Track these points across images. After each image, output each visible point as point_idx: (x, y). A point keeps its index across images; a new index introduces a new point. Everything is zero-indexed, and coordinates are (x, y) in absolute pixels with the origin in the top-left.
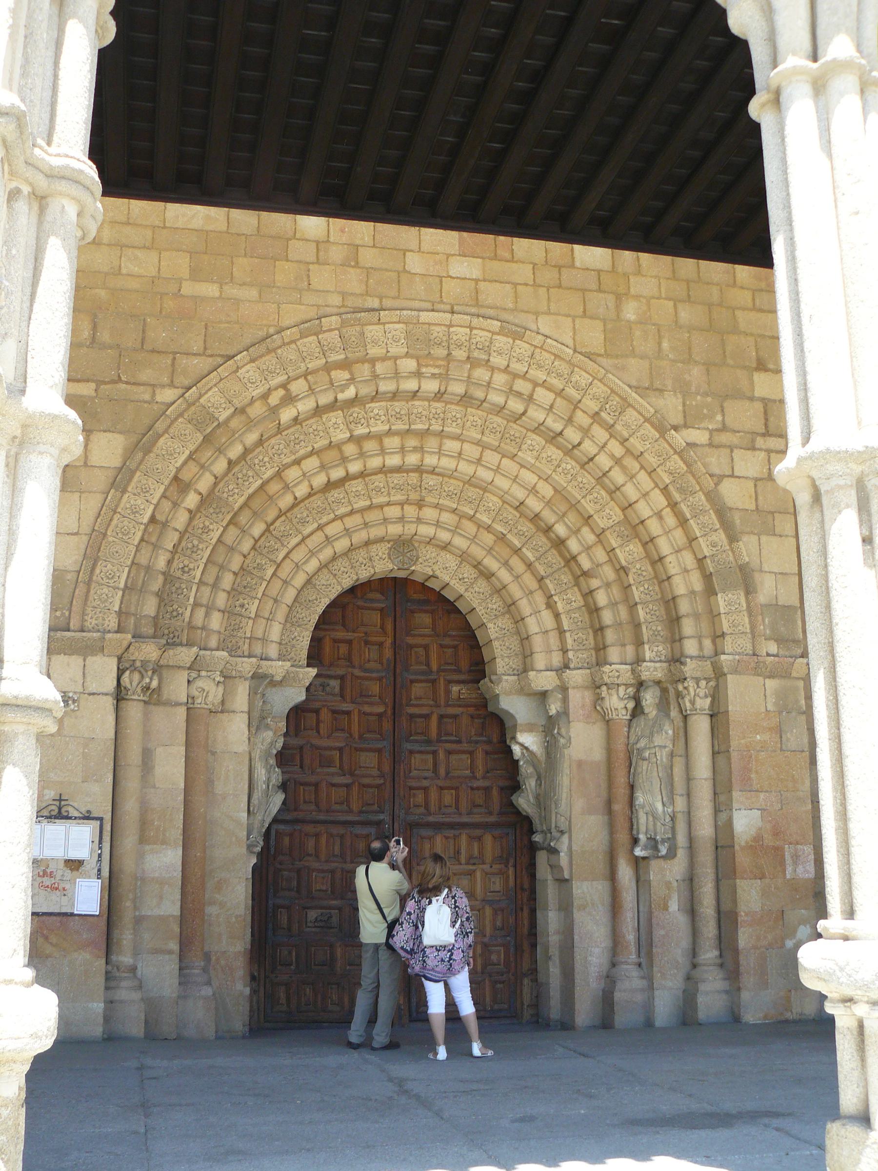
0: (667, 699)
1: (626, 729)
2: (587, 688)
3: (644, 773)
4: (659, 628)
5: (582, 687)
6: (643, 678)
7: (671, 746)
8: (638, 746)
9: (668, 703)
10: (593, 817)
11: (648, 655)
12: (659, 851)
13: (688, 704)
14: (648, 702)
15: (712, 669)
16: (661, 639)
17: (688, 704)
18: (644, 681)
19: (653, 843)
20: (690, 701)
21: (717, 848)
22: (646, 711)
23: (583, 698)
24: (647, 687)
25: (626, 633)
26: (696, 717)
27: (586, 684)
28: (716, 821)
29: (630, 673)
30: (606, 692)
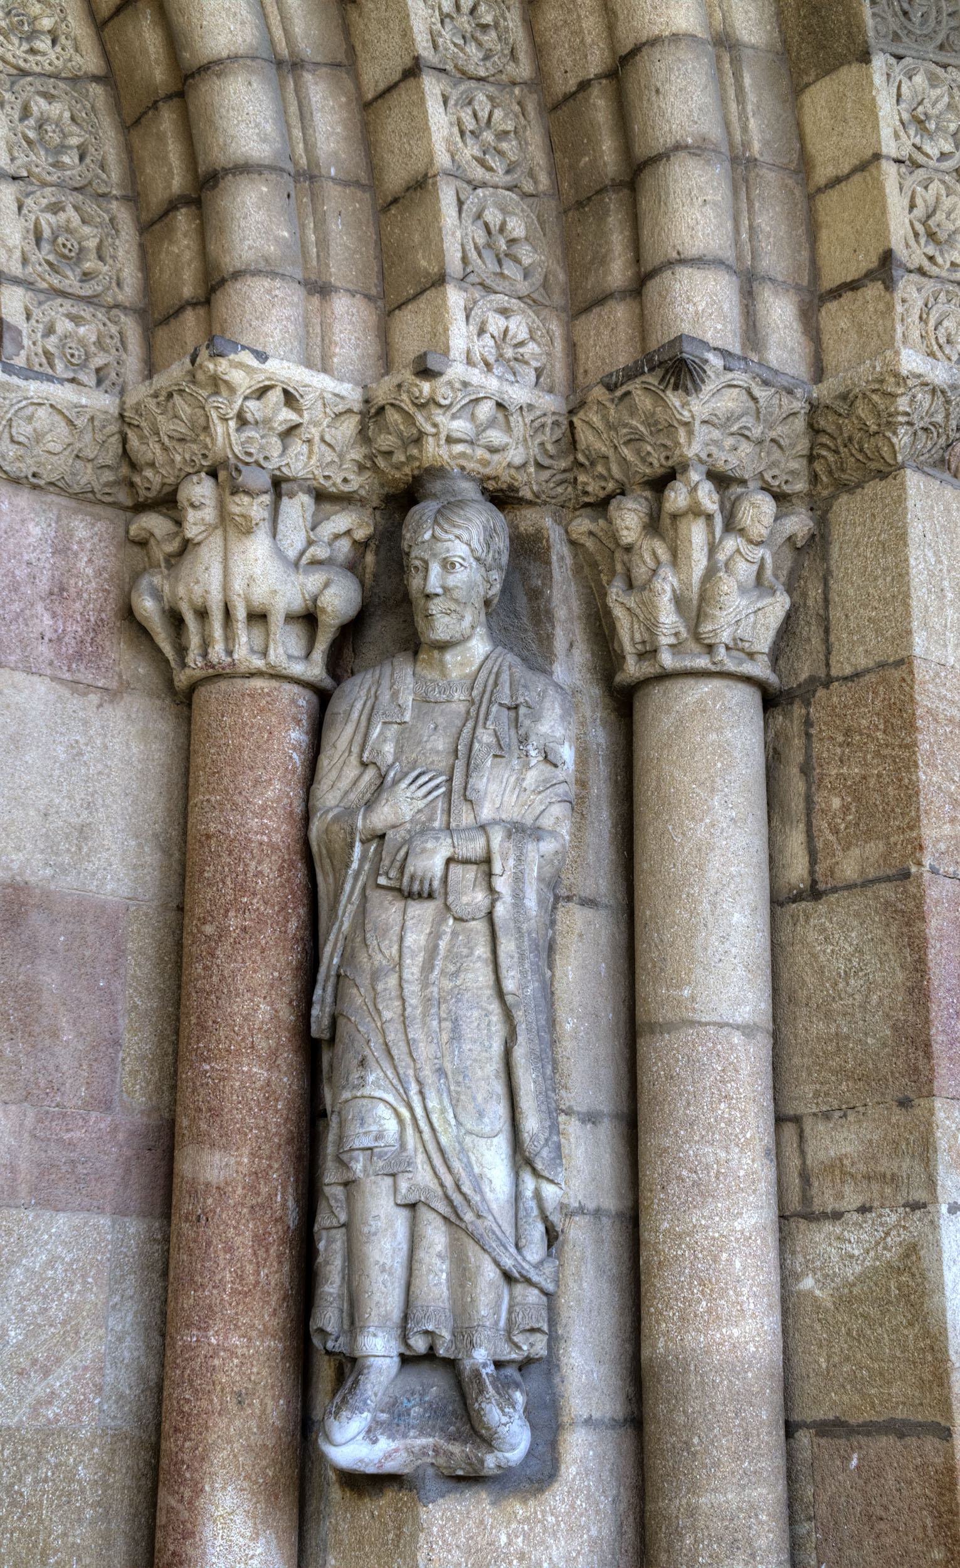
0: (535, 595)
1: (297, 736)
2: (85, 498)
3: (412, 969)
4: (517, 227)
5: (57, 487)
6: (434, 451)
7: (565, 830)
8: (382, 816)
9: (541, 617)
10: (62, 1222)
11: (459, 336)
12: (485, 1439)
13: (668, 618)
14: (459, 578)
15: (803, 446)
16: (523, 287)
17: (668, 618)
18: (436, 472)
19: (436, 1385)
20: (679, 601)
21: (790, 1429)
22: (443, 627)
23: (61, 549)
24: (451, 506)
25: (336, 226)
26: (706, 687)
27: (86, 476)
28: (787, 1278)
29: (349, 427)
30: (209, 514)
